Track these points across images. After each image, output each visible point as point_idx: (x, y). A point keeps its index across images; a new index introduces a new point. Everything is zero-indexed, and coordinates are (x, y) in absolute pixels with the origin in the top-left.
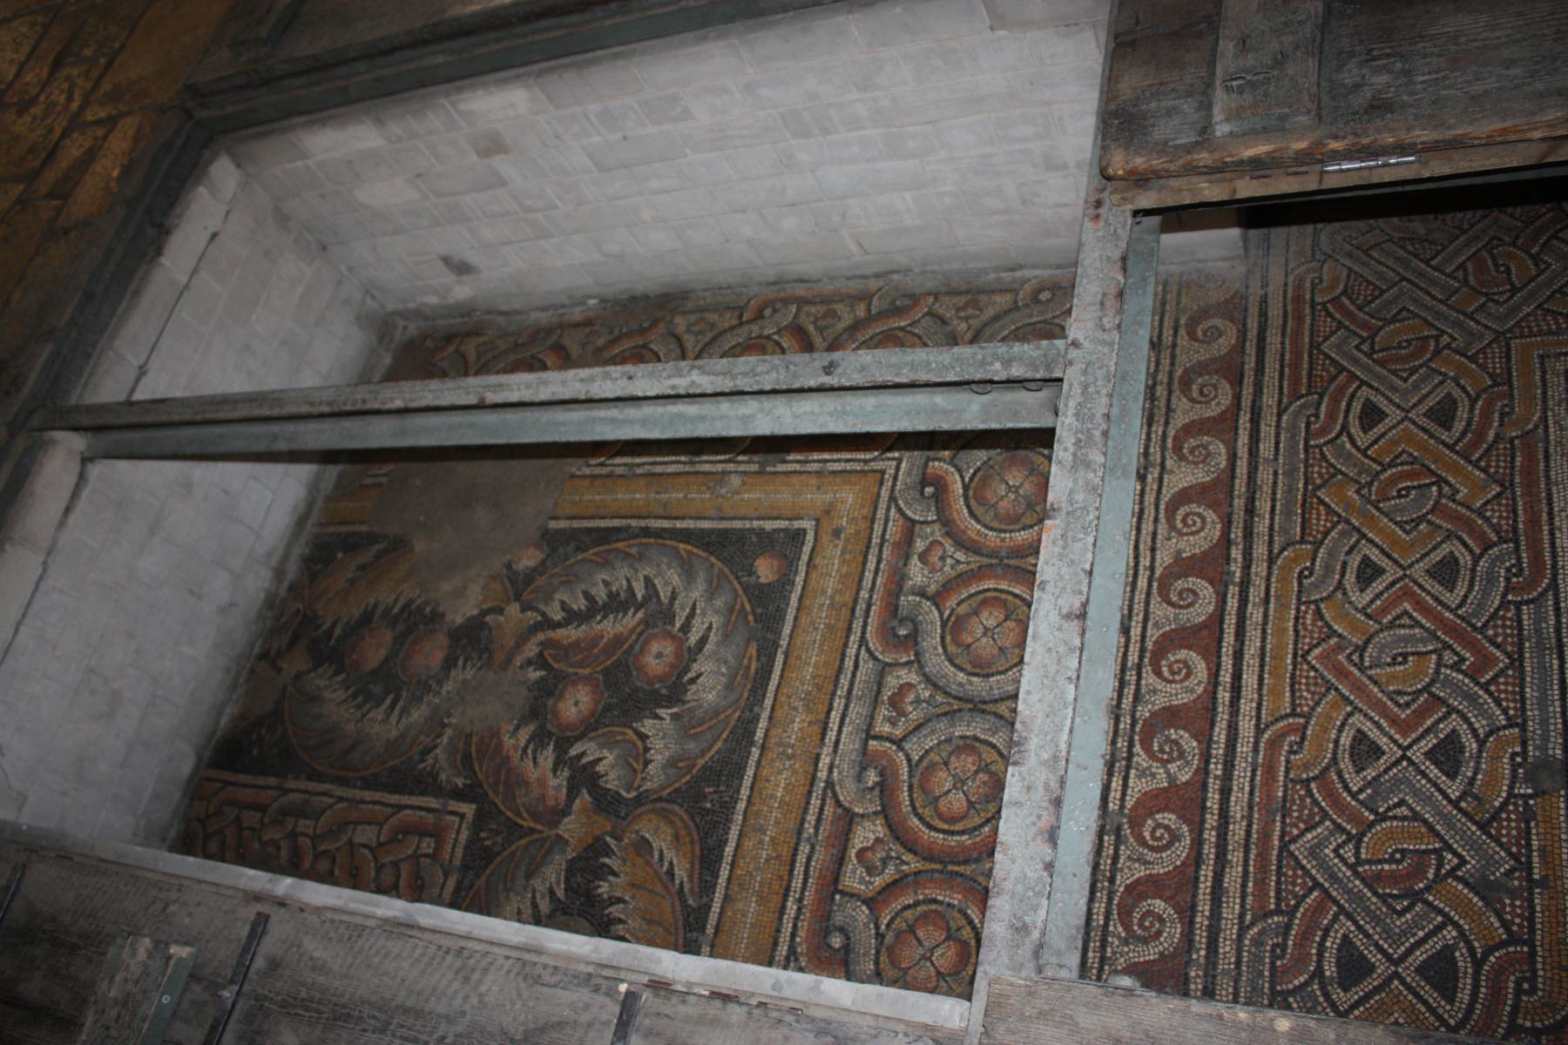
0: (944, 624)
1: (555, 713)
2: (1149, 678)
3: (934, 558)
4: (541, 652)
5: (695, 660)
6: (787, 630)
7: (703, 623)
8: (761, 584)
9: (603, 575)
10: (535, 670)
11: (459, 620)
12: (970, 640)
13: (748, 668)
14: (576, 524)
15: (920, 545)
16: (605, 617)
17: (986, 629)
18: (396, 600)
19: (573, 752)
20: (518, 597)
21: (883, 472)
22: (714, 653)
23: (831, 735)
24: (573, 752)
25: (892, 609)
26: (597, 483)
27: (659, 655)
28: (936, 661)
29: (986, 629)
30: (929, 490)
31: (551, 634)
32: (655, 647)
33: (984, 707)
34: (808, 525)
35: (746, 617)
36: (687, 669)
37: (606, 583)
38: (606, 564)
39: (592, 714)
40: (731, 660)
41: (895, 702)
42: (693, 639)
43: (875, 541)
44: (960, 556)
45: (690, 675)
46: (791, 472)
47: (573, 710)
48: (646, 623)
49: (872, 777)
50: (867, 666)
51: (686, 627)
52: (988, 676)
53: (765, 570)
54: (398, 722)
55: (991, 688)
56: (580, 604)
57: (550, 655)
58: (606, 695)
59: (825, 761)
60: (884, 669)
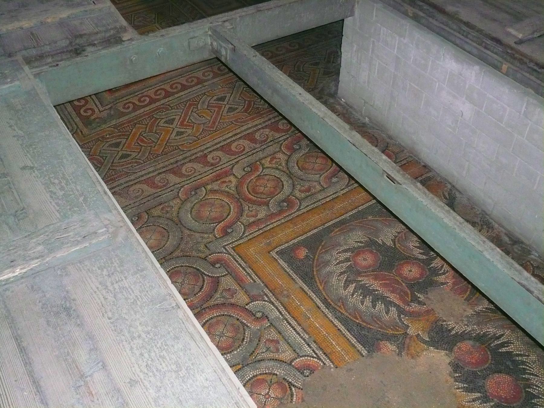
0: (273, 197)
1: (422, 275)
2: (247, 150)
3: (253, 213)
4: (411, 302)
5: (354, 247)
6: (315, 231)
7: (340, 256)
8: (308, 250)
9: (363, 308)
10: (419, 298)
11: (443, 353)
12: (272, 189)
13: (339, 231)
14: (353, 341)
15: (252, 220)
16: (374, 291)
17: (265, 188)
18: (474, 400)
19: (425, 257)
20: (406, 334)
21: (233, 248)
22: (345, 244)
23: (334, 196)
24: (425, 257)
25: (281, 212)
26: (328, 351)
27: (365, 259)
28: (287, 189)
29: (265, 188)
30: (229, 231)
31: (402, 305)
32: (364, 263)
33: (289, 173)
34: (273, 254)
35: (324, 245)
36: (360, 247)
37: (362, 303)
38: (356, 309)
39: (408, 263)
40: (342, 238)
41: (308, 190)
42: (348, 254)
43: (261, 231)
44: (247, 208)
45: (360, 245)
46: (257, 276)
47: (413, 270)
48: (359, 274)
49: (334, 180)
50: (304, 204)
51: (347, 260)
52: (279, 178)
53: (303, 253)
54: (502, 335)
55: (282, 175)
56: (380, 306)
57: (408, 297)
58: (396, 264)
59: (342, 192)
60: (301, 200)
